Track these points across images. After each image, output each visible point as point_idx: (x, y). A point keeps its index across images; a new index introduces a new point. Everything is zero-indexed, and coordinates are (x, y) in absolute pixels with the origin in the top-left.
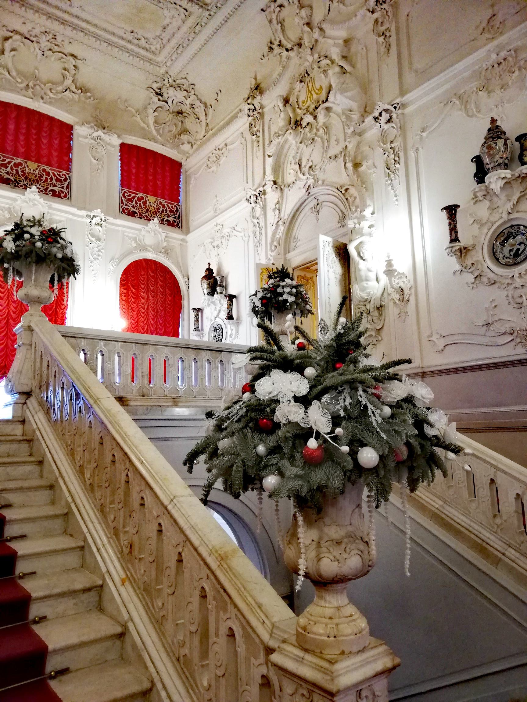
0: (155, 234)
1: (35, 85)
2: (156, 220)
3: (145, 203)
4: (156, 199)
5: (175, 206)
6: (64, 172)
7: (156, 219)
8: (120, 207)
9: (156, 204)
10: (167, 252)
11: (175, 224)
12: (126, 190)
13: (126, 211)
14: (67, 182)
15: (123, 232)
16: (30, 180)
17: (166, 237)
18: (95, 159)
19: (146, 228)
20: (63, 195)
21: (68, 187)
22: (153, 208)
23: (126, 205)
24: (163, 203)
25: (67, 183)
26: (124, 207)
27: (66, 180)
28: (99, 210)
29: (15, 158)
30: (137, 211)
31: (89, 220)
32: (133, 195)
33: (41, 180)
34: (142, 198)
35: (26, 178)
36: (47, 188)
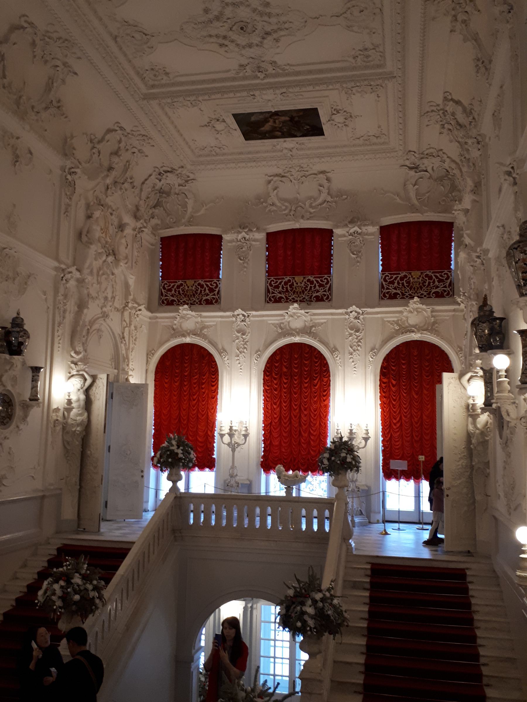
0: (418, 312)
1: (296, 208)
2: (416, 299)
3: (408, 282)
4: (422, 273)
5: (444, 274)
6: (326, 276)
7: (416, 299)
8: (381, 292)
9: (421, 278)
10: (431, 328)
11: (446, 293)
12: (387, 274)
13: (387, 295)
14: (329, 284)
15: (382, 319)
16: (297, 293)
17: (432, 312)
18: (354, 254)
19: (408, 309)
20: (325, 298)
21: (330, 289)
22: (418, 284)
23: (388, 289)
24: (430, 274)
25: (328, 286)
26: (384, 291)
27: (328, 283)
28: (354, 306)
29: (285, 277)
30: (398, 292)
31: (347, 317)
32: (395, 276)
33: (306, 290)
34: (405, 276)
35: (294, 292)
36: (312, 296)
